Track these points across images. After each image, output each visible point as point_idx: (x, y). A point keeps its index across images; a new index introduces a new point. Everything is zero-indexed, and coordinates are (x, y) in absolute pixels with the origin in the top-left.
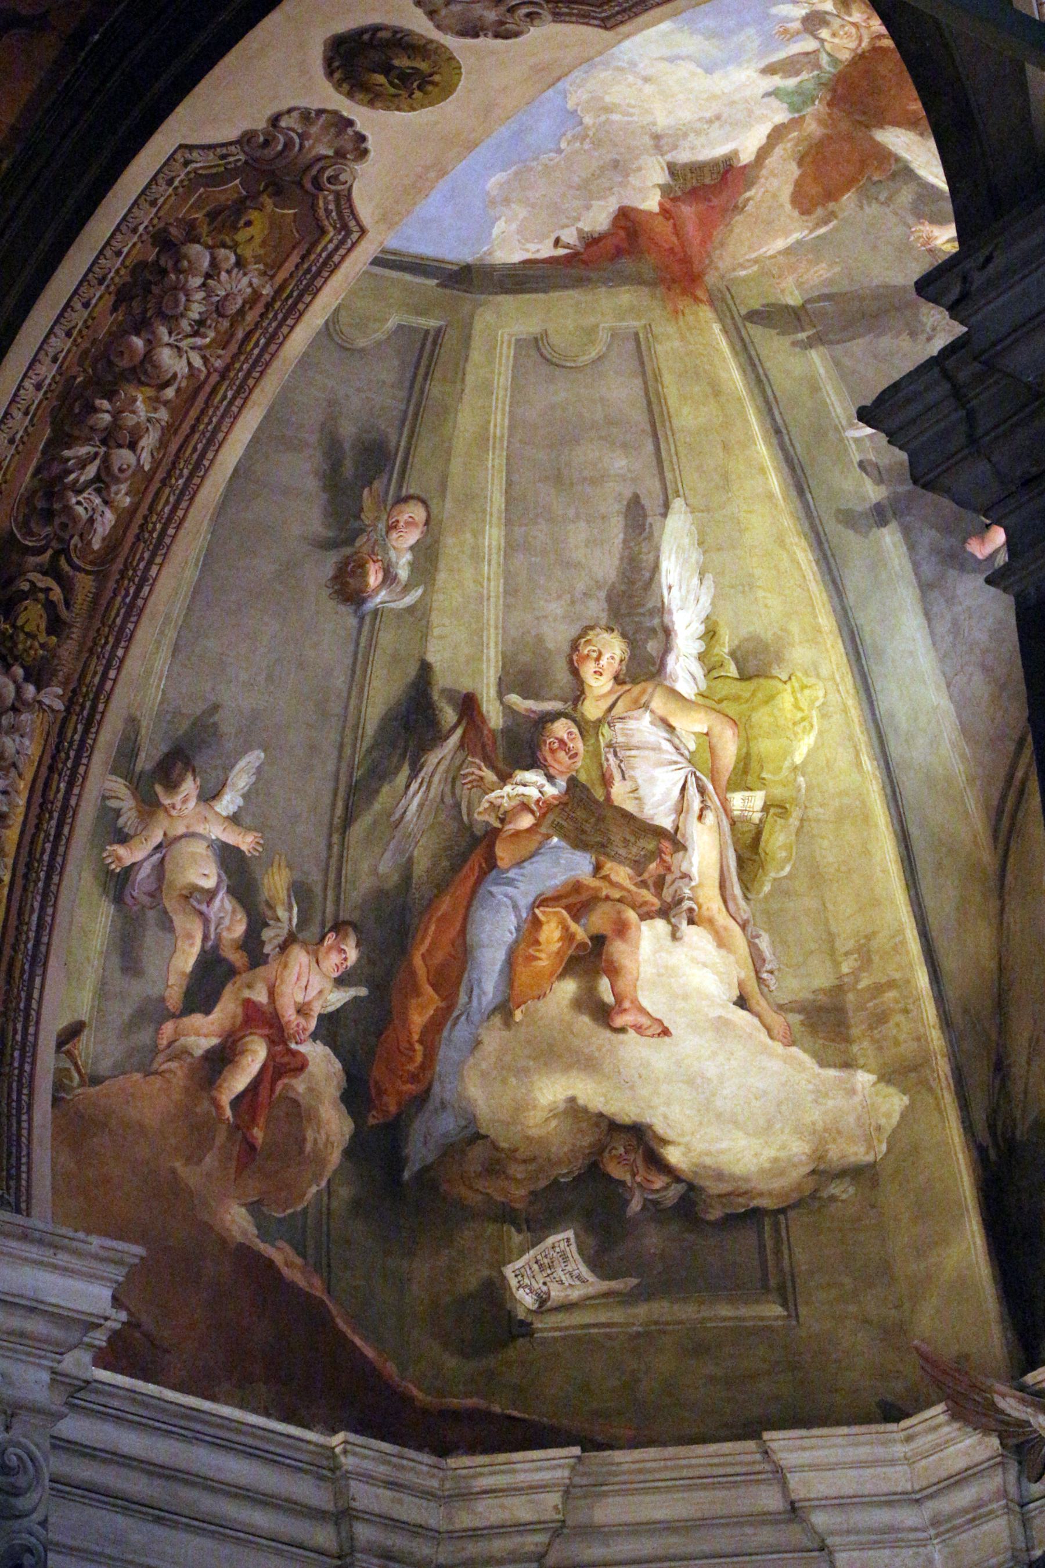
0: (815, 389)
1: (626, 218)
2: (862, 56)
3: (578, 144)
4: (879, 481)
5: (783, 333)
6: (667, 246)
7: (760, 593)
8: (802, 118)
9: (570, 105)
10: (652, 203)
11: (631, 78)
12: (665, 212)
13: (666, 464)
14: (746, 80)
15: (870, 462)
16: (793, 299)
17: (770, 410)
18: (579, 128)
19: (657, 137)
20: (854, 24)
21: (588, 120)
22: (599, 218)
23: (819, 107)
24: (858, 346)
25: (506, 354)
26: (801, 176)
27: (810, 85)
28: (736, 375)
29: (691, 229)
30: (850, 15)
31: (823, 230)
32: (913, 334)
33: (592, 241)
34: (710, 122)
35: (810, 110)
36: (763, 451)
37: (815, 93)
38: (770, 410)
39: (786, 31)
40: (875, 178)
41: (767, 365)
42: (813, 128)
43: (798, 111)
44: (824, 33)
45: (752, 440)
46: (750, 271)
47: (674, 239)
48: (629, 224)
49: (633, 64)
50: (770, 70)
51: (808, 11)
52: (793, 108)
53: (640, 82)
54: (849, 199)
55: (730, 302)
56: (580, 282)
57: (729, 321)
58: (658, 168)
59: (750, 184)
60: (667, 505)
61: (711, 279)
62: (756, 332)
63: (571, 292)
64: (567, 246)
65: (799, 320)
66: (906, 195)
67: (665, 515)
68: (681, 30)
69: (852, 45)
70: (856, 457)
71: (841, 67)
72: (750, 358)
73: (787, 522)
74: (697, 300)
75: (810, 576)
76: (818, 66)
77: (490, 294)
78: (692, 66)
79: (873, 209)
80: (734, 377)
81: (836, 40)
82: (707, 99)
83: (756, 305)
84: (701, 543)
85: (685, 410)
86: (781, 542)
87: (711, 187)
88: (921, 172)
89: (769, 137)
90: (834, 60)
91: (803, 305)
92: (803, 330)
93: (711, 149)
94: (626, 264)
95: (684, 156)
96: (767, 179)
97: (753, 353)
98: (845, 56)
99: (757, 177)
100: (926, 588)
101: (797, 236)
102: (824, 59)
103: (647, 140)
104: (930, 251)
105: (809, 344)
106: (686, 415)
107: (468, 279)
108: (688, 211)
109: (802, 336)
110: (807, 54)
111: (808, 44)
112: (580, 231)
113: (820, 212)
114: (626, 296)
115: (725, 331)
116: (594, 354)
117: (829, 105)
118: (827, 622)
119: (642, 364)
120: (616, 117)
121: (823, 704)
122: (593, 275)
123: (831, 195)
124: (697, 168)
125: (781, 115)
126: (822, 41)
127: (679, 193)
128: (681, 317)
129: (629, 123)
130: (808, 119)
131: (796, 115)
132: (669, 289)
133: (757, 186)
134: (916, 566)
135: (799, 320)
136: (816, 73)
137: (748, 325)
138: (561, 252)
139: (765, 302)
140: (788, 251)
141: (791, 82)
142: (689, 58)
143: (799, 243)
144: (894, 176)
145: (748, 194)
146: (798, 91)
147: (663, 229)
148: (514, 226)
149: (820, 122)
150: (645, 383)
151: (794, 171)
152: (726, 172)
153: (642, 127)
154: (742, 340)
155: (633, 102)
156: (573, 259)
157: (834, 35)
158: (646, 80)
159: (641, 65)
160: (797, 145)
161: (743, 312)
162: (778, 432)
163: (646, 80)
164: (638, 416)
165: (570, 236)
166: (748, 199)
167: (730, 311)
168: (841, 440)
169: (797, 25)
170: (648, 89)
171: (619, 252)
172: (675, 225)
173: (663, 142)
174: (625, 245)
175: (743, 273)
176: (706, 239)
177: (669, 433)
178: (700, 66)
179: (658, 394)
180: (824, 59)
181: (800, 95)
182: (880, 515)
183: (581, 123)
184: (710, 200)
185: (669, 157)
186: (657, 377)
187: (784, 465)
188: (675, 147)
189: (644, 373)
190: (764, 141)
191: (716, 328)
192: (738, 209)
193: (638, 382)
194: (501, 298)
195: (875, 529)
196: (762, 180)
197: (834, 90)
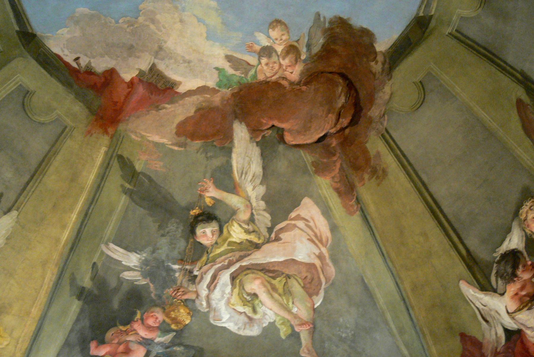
0: (111, 212)
1: (111, 73)
2: (267, 83)
3: (126, 26)
4: (93, 279)
5: (123, 177)
6: (116, 100)
7: (12, 281)
8: (218, 91)
9: (141, 6)
10: (127, 76)
11: (176, 15)
12: (131, 84)
13: (25, 192)
14: (216, 55)
15: (97, 266)
16: (139, 167)
17: (91, 203)
18: (134, 19)
19: (160, 48)
20: (280, 65)
21: (141, 19)
22: (101, 65)
23: (227, 92)
24: (140, 211)
25: (11, 86)
26: (192, 116)
27: (235, 79)
28: (92, 177)
29: (135, 98)
30: (284, 59)
31: (176, 148)
32: (160, 227)
33: (90, 72)
34: (185, 61)
35: (224, 90)
36: (73, 218)
37: (233, 84)
38: (91, 203)
39: (251, 47)
40: (215, 143)
41: (107, 184)
42: (217, 100)
43: (220, 87)
44: (264, 60)
45: (71, 210)
46: (137, 139)
47: (123, 98)
48: (109, 78)
49: (184, 10)
50: (229, 58)
51: (269, 44)
52: (220, 84)
53: (178, 20)
54: (198, 143)
55: (119, 143)
56: (67, 84)
57: (112, 150)
58: (148, 62)
59: (171, 102)
60: (9, 210)
61: (121, 127)
62: (115, 164)
63: (60, 86)
64: (78, 64)
65: (133, 177)
66: (217, 162)
67: (5, 213)
68: (217, 10)
69: (268, 75)
70: (95, 260)
71: (254, 81)
72: (105, 173)
73: (56, 256)
74: (106, 132)
75: (45, 287)
76: (246, 74)
77: (31, 55)
78: (203, 30)
79: (201, 157)
80: (90, 177)
81: (265, 68)
82: (194, 50)
83: (125, 154)
84: (7, 239)
85: (53, 177)
86: (44, 264)
87: (158, 88)
88: (234, 156)
89: (198, 88)
90: (255, 76)
91: (139, 173)
92: (130, 183)
93: (172, 74)
94: (91, 94)
95: (161, 67)
96: (179, 106)
97: (107, 173)
98: (261, 77)
99: (177, 102)
100: (67, 344)
101: (165, 141)
102: (252, 72)
103: (156, 47)
104: (200, 196)
105: (125, 191)
106: (52, 180)
107: (29, 39)
108: (141, 90)
109: (127, 186)
110: (249, 64)
111: (252, 60)
112: (90, 63)
113: (183, 139)
114: (78, 108)
115: (106, 153)
116: (42, 120)
117: (233, 95)
118: (36, 312)
119: (57, 141)
120: (152, 27)
121: (3, 348)
122: (76, 87)
123: (193, 136)
124: (160, 76)
125: (211, 84)
126: (260, 63)
127: (145, 80)
128: (88, 137)
129: (155, 34)
130: (219, 94)
131: (217, 88)
132: (96, 120)
133: (173, 105)
134: (71, 331)
135: (133, 177)
136: (243, 75)
137: (116, 159)
138: (74, 65)
139: (129, 157)
140: (157, 145)
141: (230, 71)
142: (207, 26)
143: (163, 145)
144: (222, 148)
145: (167, 106)
146: (229, 78)
147: (121, 92)
148: (69, 36)
149: (222, 98)
150: (49, 151)
151: (191, 112)
152: (169, 88)
153: (159, 40)
154: (109, 164)
155: (167, 26)
156: (74, 72)
157: (267, 64)
158: (181, 21)
159: (186, 13)
160: (203, 102)
161: (119, 153)
162: (86, 215)
163: (181, 21)
164: (34, 162)
165: (84, 62)
166: (164, 108)
167: (116, 147)
168: (98, 245)
169: (258, 48)
170: (178, 26)
171: (94, 87)
172: (130, 92)
173: (162, 53)
174: (99, 85)
175: (133, 137)
176: (135, 109)
177: (38, 181)
178: (207, 33)
179: (50, 159)
180: (252, 72)
181: (228, 80)
182: (81, 294)
183: (137, 18)
184: (152, 94)
185: (156, 61)
186: (56, 153)
187: (76, 231)
188: (162, 59)
189: (53, 146)
190: (194, 89)
191: (103, 149)
192: (158, 109)
193: (47, 148)
194: (34, 62)
195: (75, 297)
196: (177, 105)
197: (241, 90)
